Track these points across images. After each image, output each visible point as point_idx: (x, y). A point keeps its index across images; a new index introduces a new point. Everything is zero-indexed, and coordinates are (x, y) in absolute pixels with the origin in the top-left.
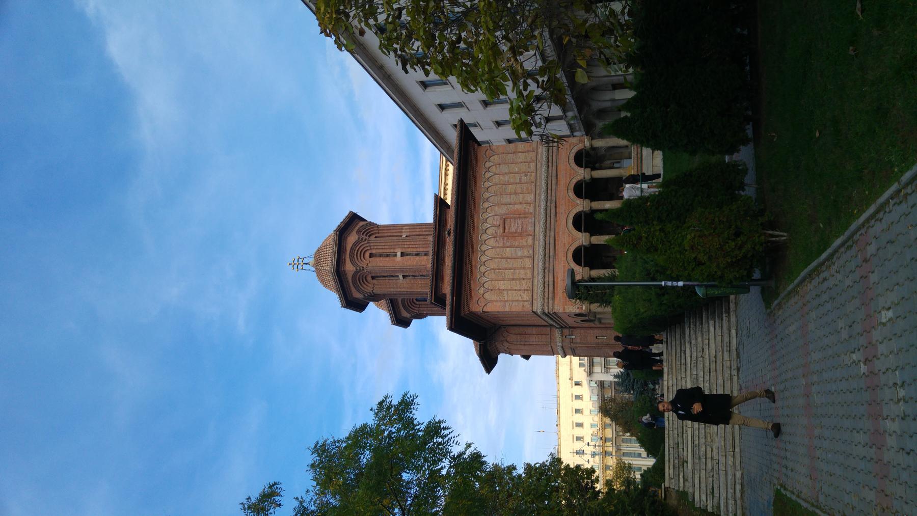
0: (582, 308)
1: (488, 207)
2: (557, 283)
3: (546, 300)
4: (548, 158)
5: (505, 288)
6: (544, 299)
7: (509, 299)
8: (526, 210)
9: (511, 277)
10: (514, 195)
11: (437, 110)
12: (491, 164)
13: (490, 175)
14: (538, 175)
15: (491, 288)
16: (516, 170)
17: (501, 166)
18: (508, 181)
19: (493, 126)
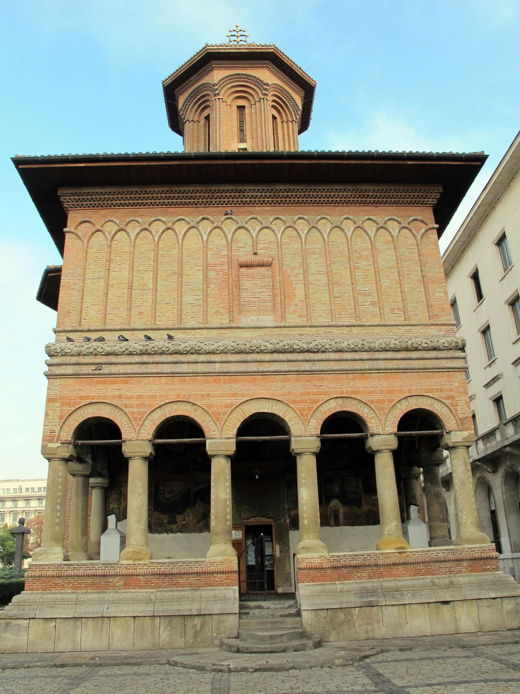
0: (51, 441)
1: (296, 230)
2: (115, 383)
3: (74, 360)
4: (417, 349)
5: (113, 274)
6: (79, 354)
7: (87, 282)
8: (292, 309)
9: (135, 284)
10: (326, 282)
11: (495, 235)
12: (395, 233)
13: (369, 232)
14: (376, 330)
15: (113, 246)
16: (385, 283)
17: (392, 252)
18: (358, 268)
19: (481, 325)
